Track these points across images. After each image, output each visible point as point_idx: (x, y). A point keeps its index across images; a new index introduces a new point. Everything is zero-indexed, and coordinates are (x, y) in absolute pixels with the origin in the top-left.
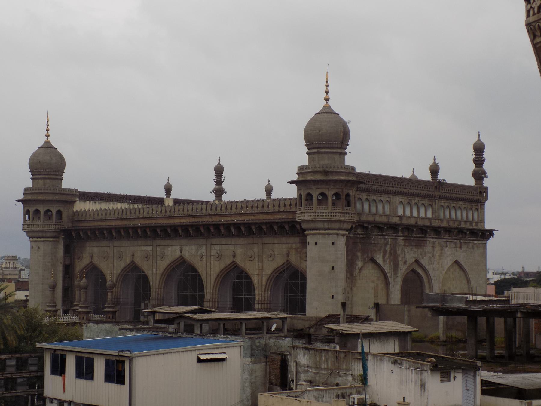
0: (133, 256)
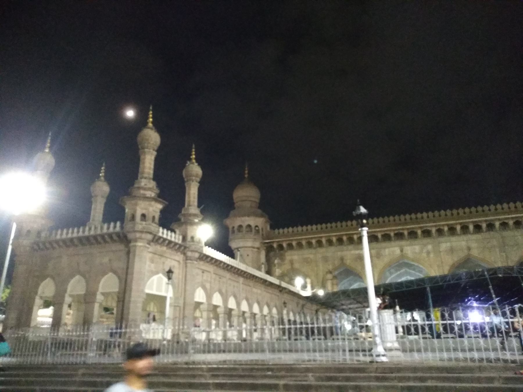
0: (342, 259)
